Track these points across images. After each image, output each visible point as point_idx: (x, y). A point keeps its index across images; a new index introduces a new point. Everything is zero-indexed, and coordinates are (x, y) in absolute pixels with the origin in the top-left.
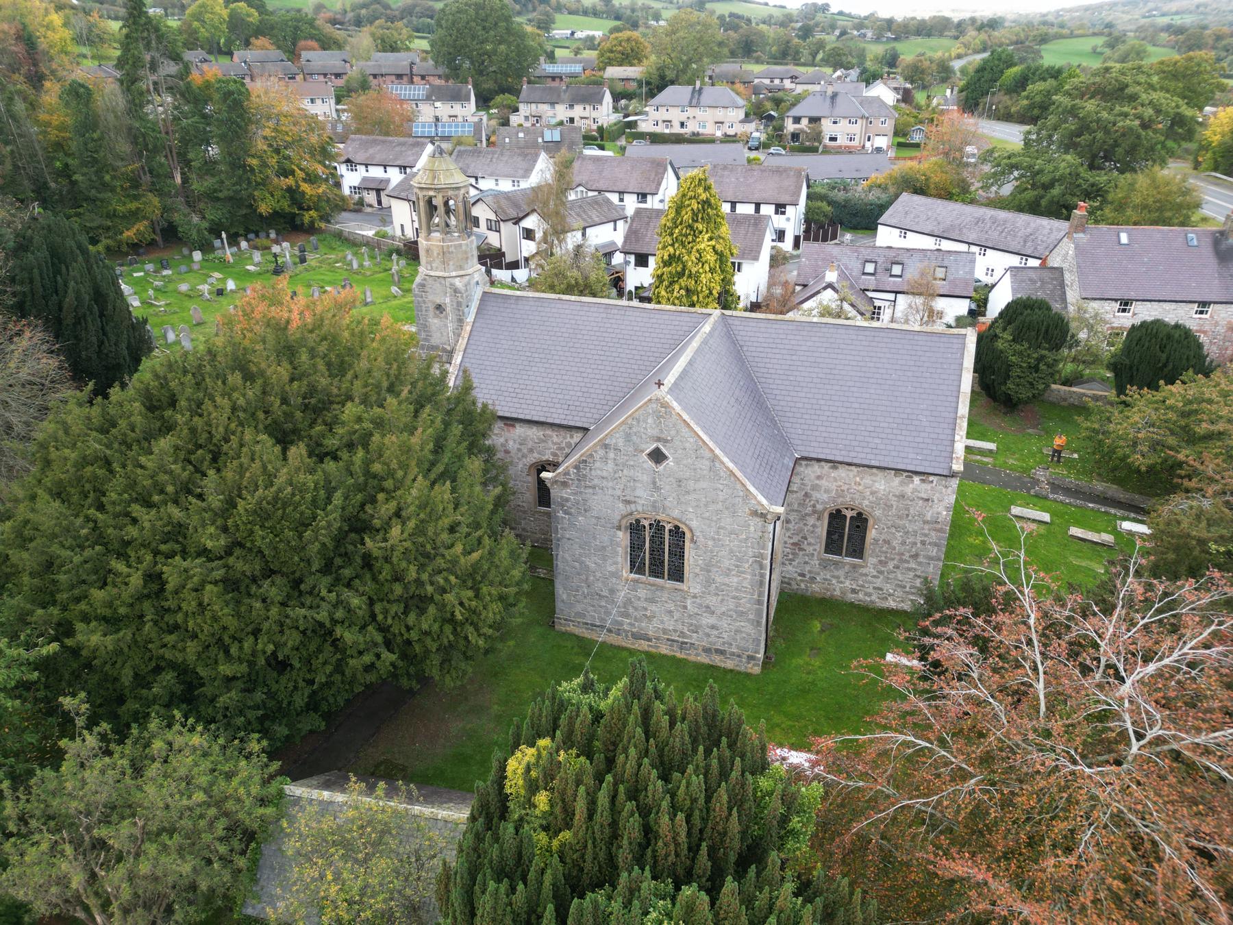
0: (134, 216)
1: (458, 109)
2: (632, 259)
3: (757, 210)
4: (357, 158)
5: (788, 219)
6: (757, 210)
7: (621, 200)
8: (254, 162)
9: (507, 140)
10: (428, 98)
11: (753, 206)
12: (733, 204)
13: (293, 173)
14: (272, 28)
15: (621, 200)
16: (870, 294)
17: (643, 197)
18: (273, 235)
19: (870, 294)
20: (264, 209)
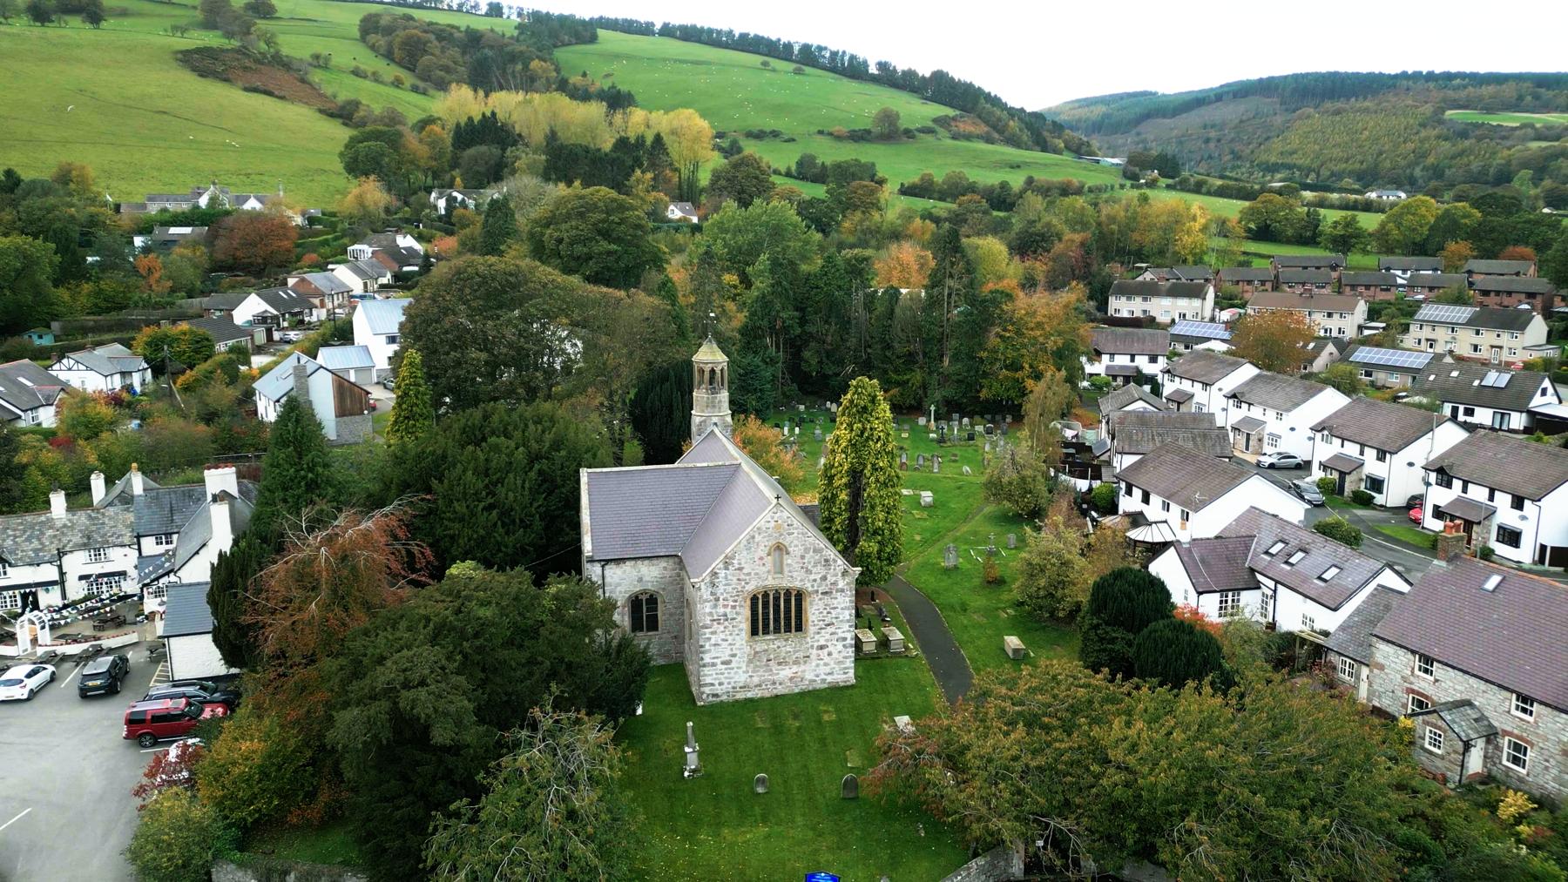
0: (898, 384)
1: (1506, 339)
2: (1123, 485)
3: (1491, 498)
4: (1179, 371)
5: (1524, 518)
6: (1491, 498)
7: (1362, 453)
8: (984, 354)
9: (1432, 378)
10: (1470, 323)
11: (1487, 491)
12: (1465, 484)
13: (1022, 368)
14: (1492, 230)
15: (1362, 453)
16: (1260, 577)
17: (1382, 455)
18: (1009, 419)
19: (1260, 577)
20: (984, 394)
